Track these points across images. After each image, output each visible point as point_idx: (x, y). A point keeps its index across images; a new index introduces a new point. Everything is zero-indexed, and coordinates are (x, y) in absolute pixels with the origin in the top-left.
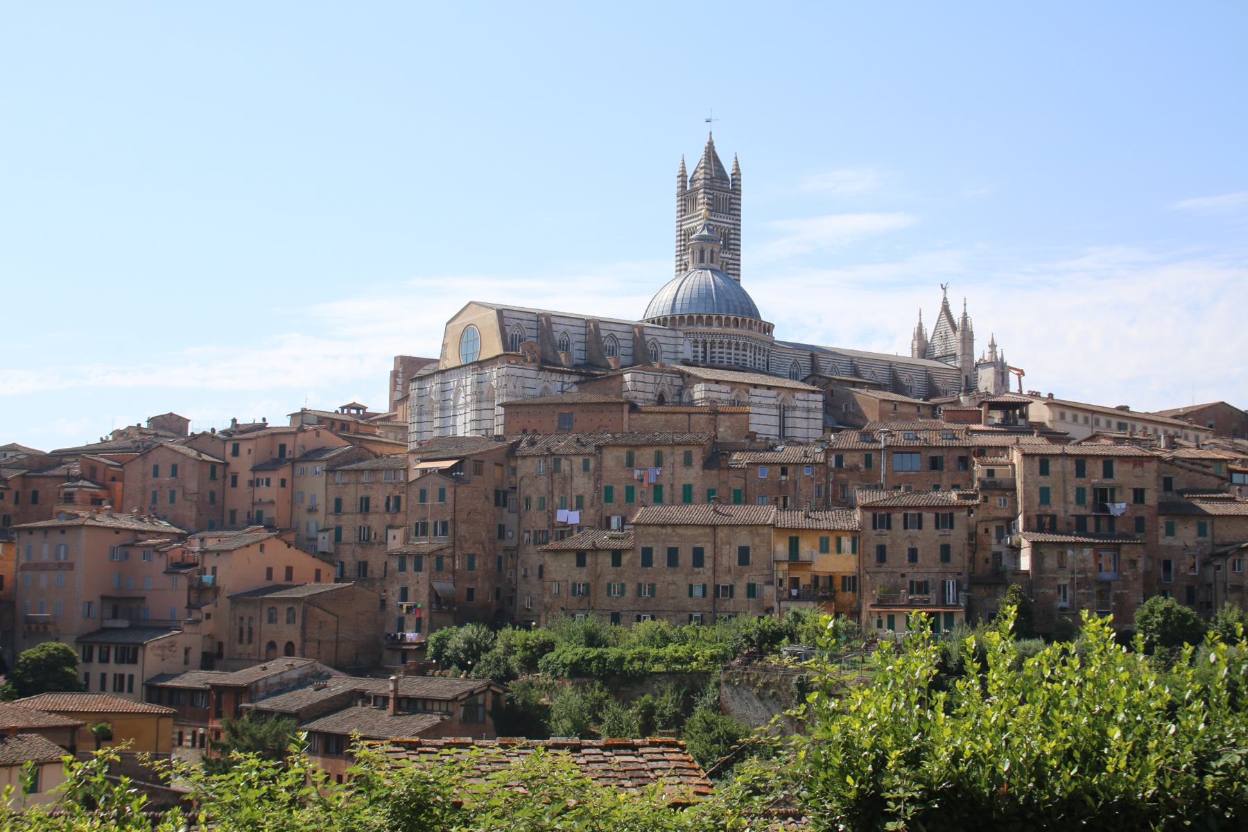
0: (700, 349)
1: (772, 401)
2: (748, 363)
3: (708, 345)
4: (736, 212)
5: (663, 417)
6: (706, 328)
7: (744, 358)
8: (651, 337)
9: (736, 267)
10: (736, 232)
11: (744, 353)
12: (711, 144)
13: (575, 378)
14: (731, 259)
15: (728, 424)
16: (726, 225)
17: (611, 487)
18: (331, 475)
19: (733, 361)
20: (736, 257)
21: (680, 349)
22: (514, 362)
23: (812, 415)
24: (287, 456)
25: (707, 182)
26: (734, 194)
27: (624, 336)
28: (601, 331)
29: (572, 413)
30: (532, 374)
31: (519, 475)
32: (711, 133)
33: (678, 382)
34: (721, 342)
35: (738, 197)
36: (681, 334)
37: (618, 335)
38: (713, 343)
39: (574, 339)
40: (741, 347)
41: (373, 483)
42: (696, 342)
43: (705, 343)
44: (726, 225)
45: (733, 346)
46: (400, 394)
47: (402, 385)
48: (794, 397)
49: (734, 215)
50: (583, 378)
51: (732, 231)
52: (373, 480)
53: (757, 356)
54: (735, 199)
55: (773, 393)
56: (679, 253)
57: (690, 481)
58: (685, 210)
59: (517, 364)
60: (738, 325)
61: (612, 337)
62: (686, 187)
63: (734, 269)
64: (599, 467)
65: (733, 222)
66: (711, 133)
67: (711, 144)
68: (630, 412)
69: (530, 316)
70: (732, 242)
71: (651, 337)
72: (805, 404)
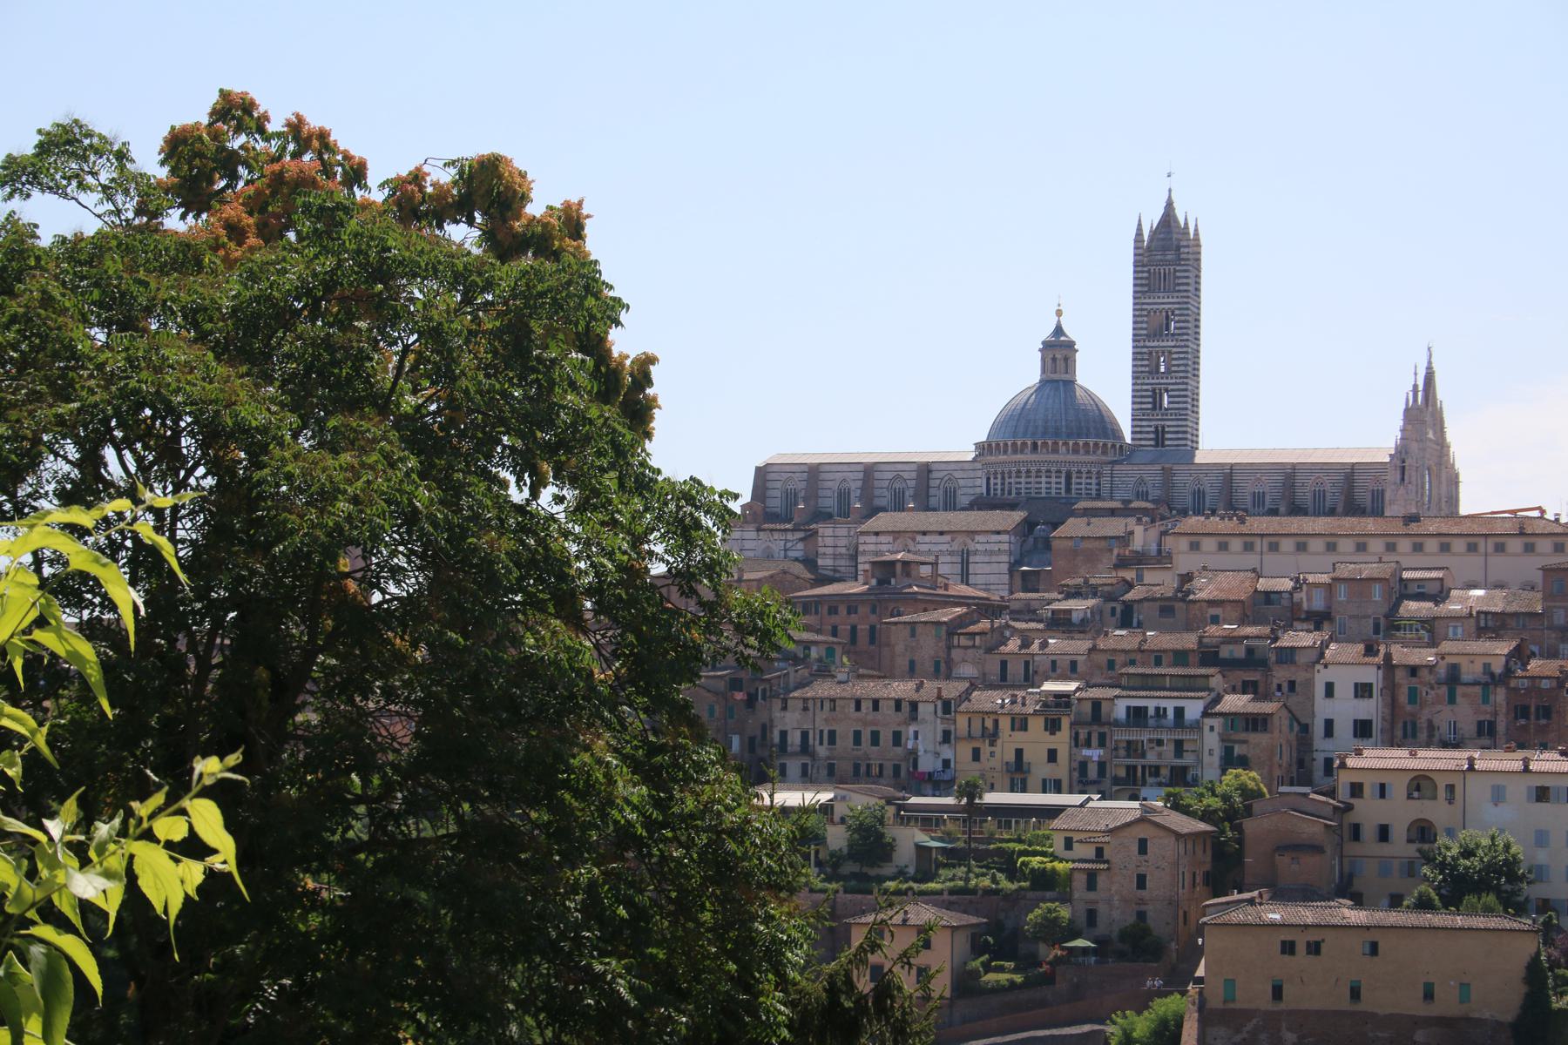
2: (1043, 491)
4: (1182, 288)
12: (1169, 205)
16: (1167, 307)
23: (994, 559)
30: (753, 535)
32: (1170, 190)
44: (1167, 307)
55: (947, 538)
65: (1175, 300)
66: (1170, 190)
67: (1169, 205)
72: (988, 547)
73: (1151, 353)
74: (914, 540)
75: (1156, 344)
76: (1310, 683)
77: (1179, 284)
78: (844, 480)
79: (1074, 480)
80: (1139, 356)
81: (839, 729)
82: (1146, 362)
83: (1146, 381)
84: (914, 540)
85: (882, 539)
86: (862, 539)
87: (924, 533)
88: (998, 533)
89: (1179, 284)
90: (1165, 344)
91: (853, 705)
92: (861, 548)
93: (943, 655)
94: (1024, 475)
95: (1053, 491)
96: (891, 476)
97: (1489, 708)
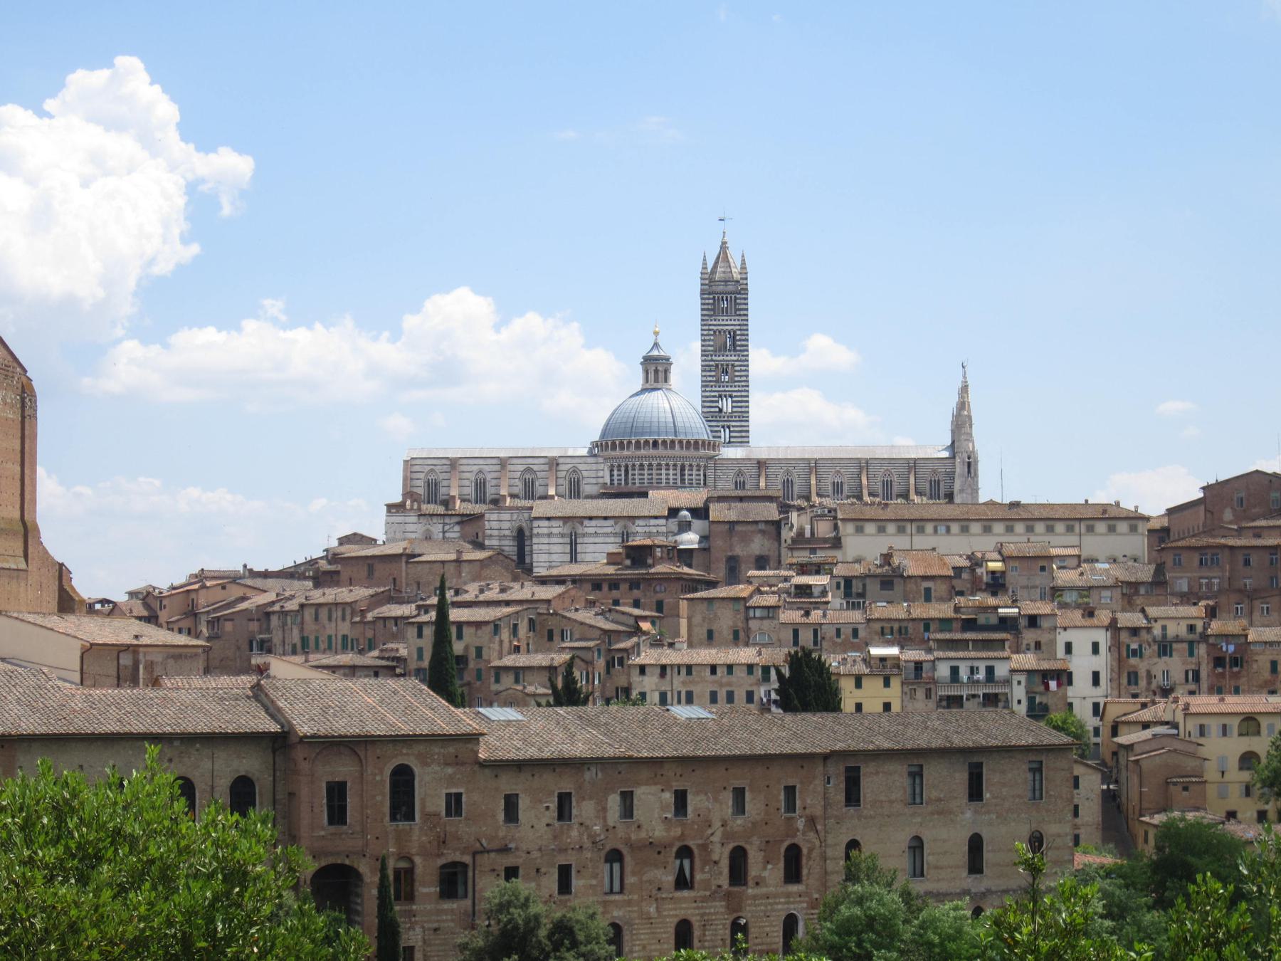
1: (609, 530)
2: (664, 481)
4: (742, 313)
5: (428, 566)
8: (571, 466)
9: (743, 368)
10: (743, 332)
12: (724, 246)
14: (737, 361)
15: (467, 570)
16: (729, 328)
19: (646, 481)
20: (744, 358)
21: (601, 474)
22: (394, 511)
25: (707, 287)
26: (740, 293)
27: (543, 467)
30: (414, 519)
35: (744, 296)
36: (601, 460)
37: (535, 468)
39: (489, 477)
40: (655, 467)
42: (612, 466)
45: (646, 467)
48: (634, 524)
49: (740, 315)
50: (465, 519)
51: (738, 332)
54: (740, 299)
55: (611, 522)
57: (345, 632)
59: (398, 512)
61: (528, 470)
63: (741, 371)
64: (302, 623)
65: (737, 322)
67: (724, 246)
68: (407, 562)
69: (444, 461)
70: (738, 343)
72: (647, 529)
73: (717, 366)
74: (582, 524)
75: (721, 358)
76: (1053, 642)
78: (480, 472)
79: (686, 472)
80: (708, 368)
81: (696, 690)
82: (713, 374)
83: (714, 389)
84: (582, 524)
85: (554, 523)
86: (536, 524)
87: (591, 518)
88: (656, 517)
90: (729, 358)
91: (708, 670)
92: (535, 531)
93: (740, 625)
94: (695, 468)
95: (671, 481)
96: (522, 468)
97: (1194, 660)
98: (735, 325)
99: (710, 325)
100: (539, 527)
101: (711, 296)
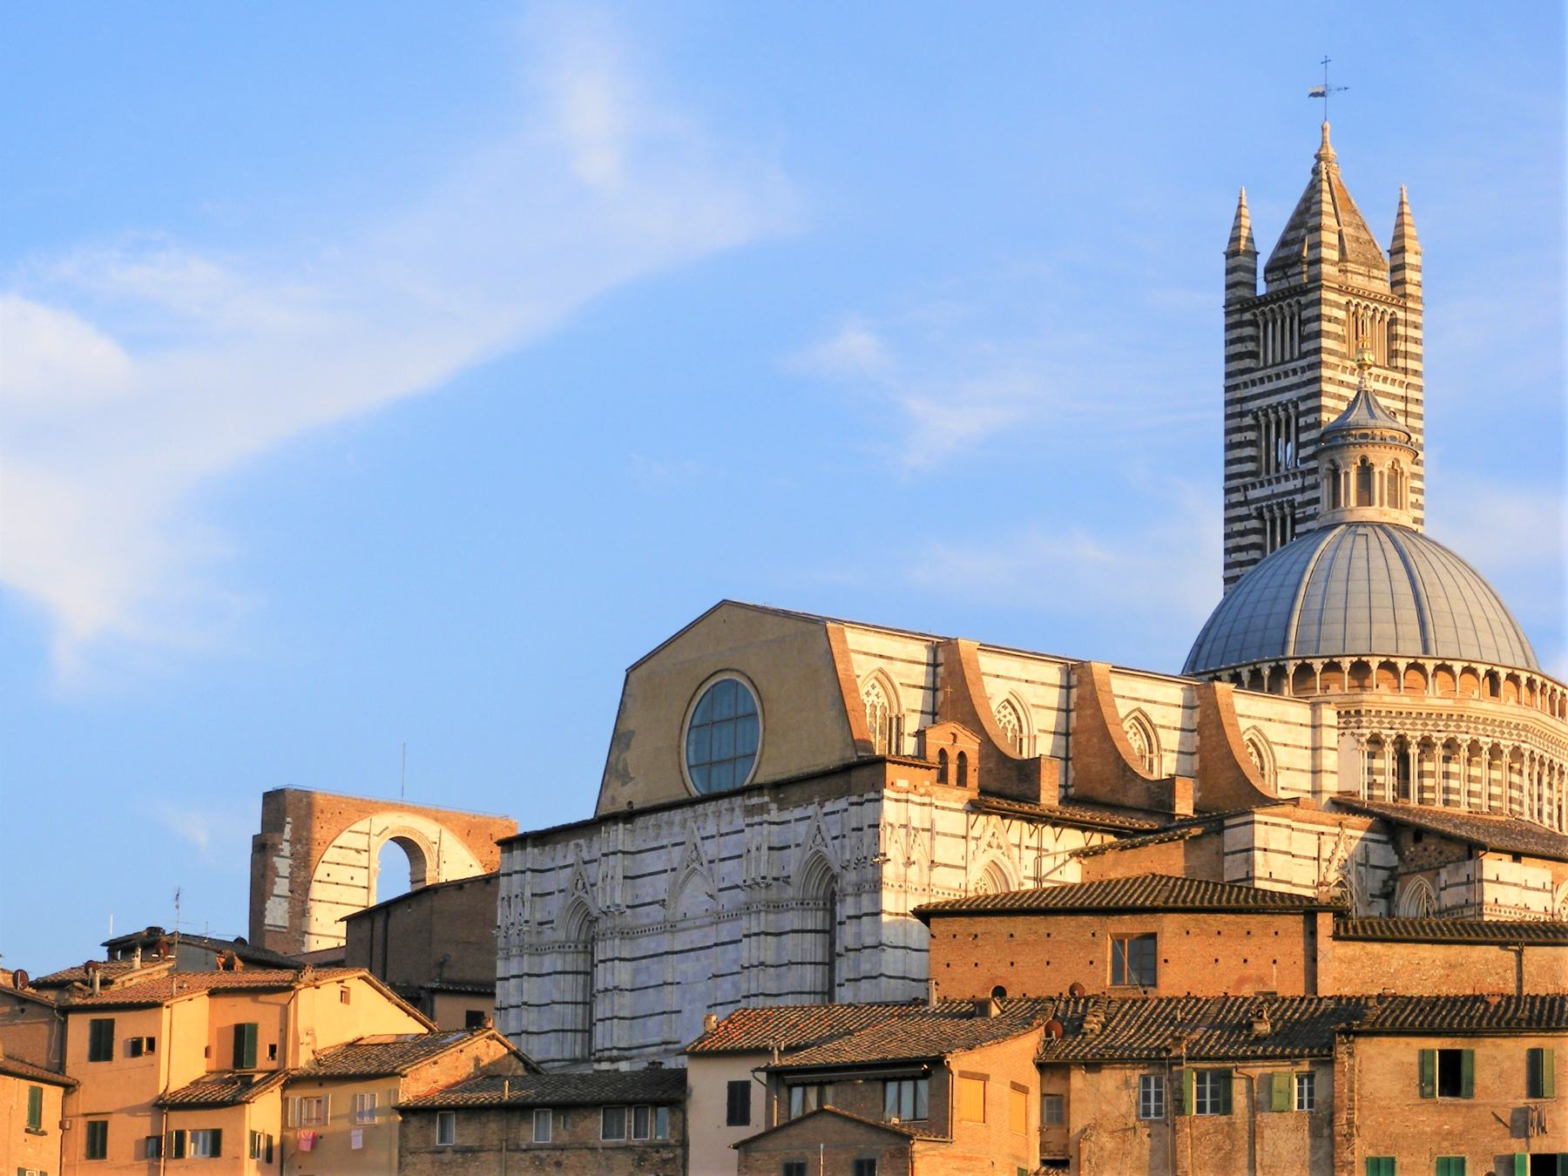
0: (1387, 762)
3: (1414, 751)
4: (1412, 364)
6: (1407, 700)
7: (1515, 794)
8: (1249, 723)
11: (1515, 778)
13: (1074, 839)
17: (1392, 1161)
18: (415, 1122)
22: (903, 783)
24: (263, 1061)
28: (1118, 701)
29: (1153, 936)
30: (954, 821)
31: (1077, 1122)
33: (1383, 855)
34: (1451, 745)
37: (1156, 715)
38: (1426, 744)
41: (563, 1149)
42: (1376, 741)
43: (1401, 744)
46: (286, 905)
47: (291, 878)
49: (1405, 371)
50: (1096, 840)
52: (565, 1138)
53: (1546, 793)
56: (1235, 483)
58: (1253, 355)
60: (1494, 691)
62: (1254, 287)
65: (1401, 392)
71: (1249, 723)
77: (1406, 355)
89: (1406, 355)
98: (1393, 397)
99: (1341, 383)
100: (1497, 881)
101: (1343, 300)
